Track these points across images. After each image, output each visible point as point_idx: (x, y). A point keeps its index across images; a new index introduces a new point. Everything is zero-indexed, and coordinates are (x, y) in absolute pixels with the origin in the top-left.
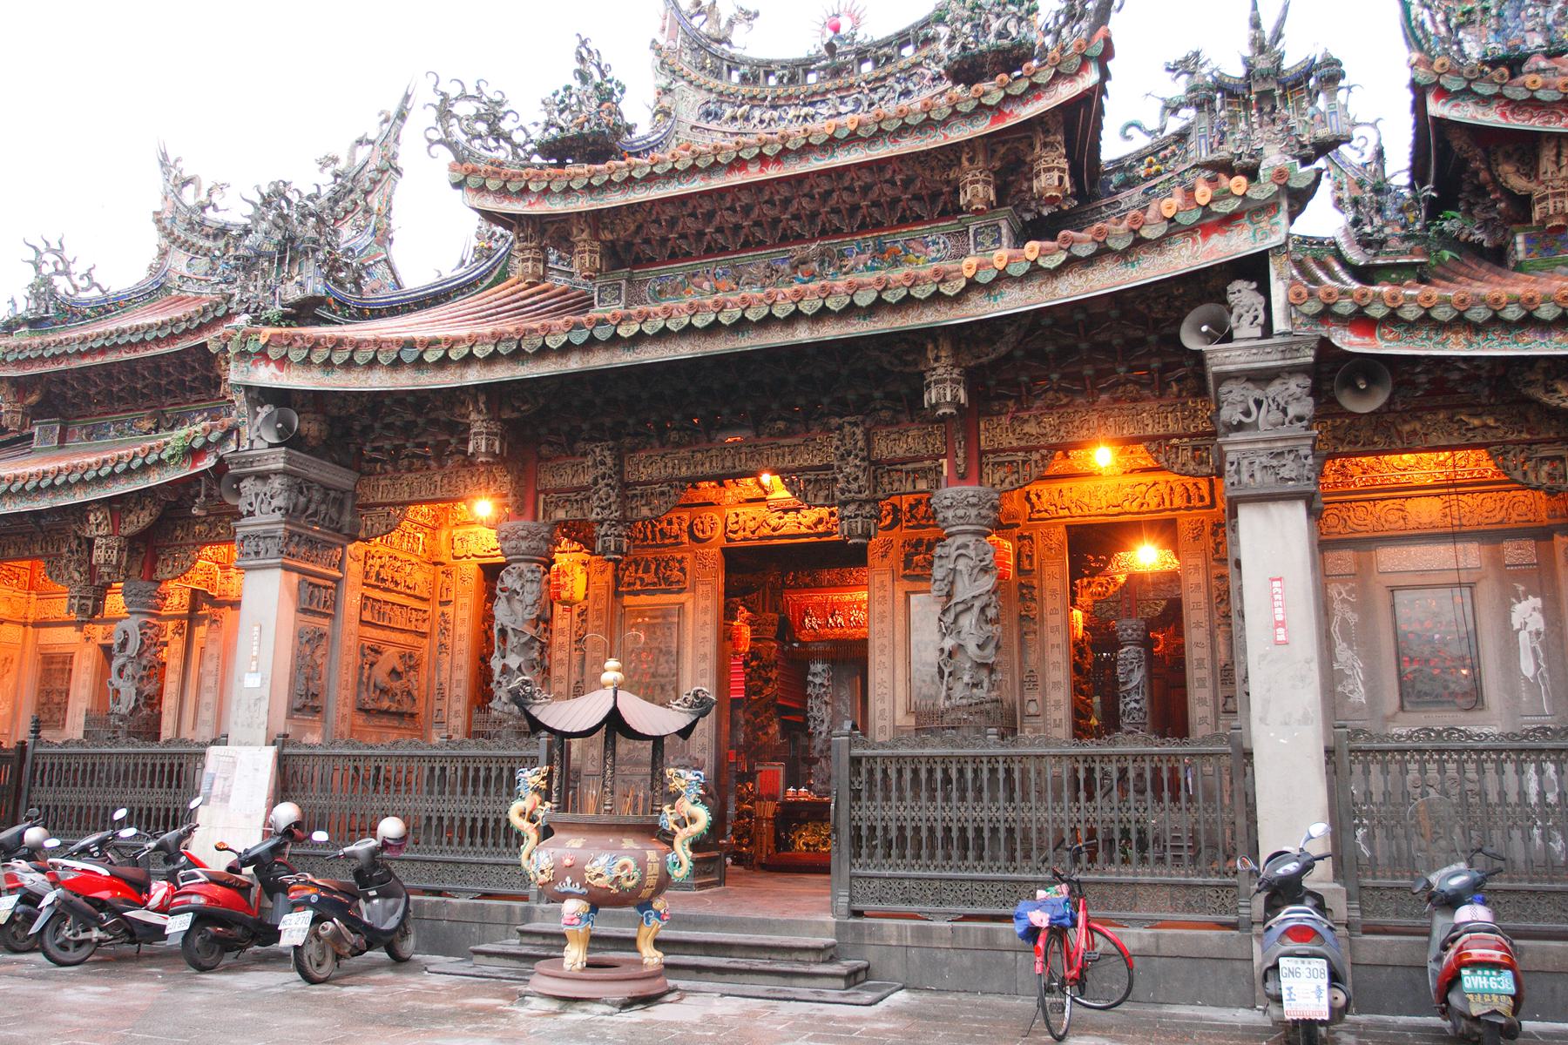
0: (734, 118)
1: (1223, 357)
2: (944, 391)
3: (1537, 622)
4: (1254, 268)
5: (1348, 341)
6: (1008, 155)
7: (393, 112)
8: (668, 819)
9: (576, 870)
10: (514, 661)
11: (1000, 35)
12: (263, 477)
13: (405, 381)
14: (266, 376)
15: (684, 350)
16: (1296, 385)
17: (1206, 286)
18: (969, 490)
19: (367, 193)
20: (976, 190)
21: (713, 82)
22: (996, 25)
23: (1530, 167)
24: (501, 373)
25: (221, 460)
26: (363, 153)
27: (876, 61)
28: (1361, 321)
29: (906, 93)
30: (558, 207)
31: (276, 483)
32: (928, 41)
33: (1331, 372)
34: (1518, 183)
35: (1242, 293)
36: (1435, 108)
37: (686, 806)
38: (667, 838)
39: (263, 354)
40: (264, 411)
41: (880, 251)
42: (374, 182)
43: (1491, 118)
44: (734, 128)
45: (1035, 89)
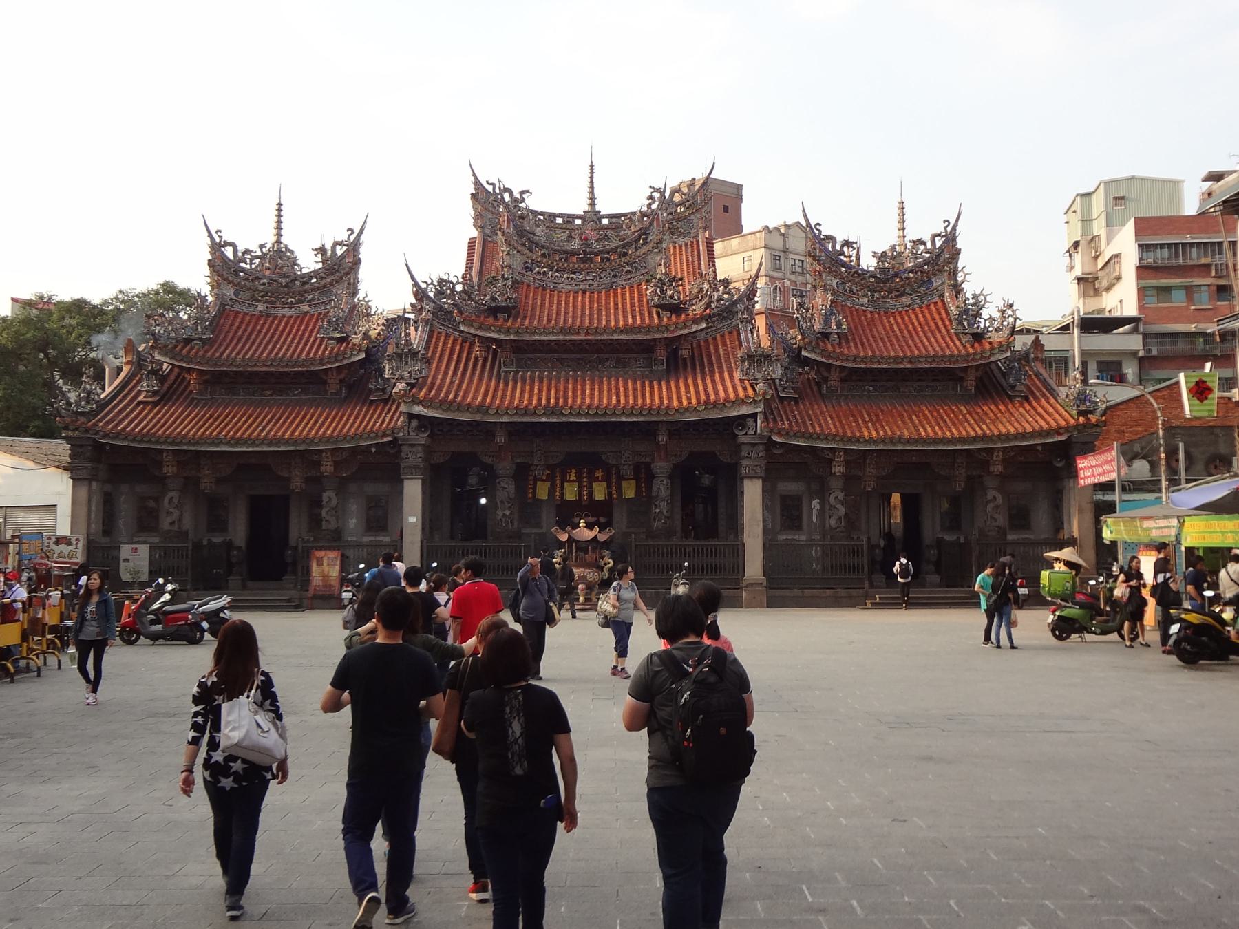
0: (539, 273)
1: (742, 438)
2: (662, 438)
3: (818, 506)
4: (754, 416)
5: (776, 439)
6: (673, 345)
7: (357, 231)
8: (602, 563)
9: (585, 577)
10: (507, 513)
11: (672, 297)
12: (413, 446)
13: (478, 418)
14: (418, 409)
15: (583, 420)
16: (761, 448)
17: (741, 421)
18: (665, 465)
19: (347, 273)
20: (662, 354)
21: (530, 254)
22: (669, 293)
23: (829, 371)
24: (515, 420)
25: (395, 439)
26: (340, 251)
27: (602, 260)
28: (779, 434)
29: (615, 276)
30: (502, 337)
31: (420, 449)
32: (625, 254)
33: (770, 444)
34: (826, 374)
35: (750, 422)
36: (804, 353)
37: (606, 559)
38: (601, 568)
39: (420, 403)
40: (414, 423)
41: (618, 361)
42: (351, 269)
43: (819, 358)
44: (540, 277)
45: (685, 327)
